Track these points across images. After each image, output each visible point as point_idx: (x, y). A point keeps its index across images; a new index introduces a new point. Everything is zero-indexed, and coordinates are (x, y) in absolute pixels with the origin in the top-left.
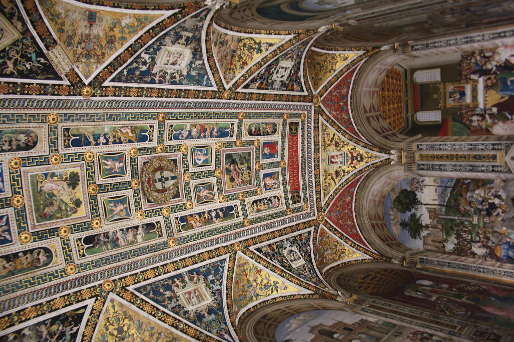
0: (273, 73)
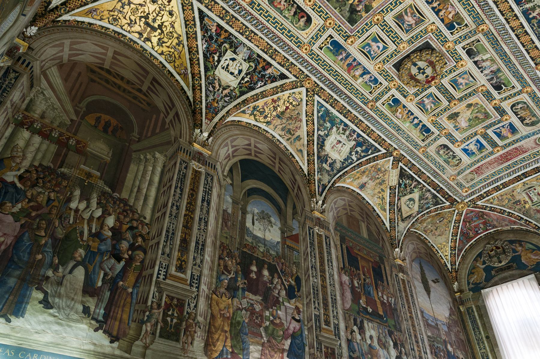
0: (247, 74)
